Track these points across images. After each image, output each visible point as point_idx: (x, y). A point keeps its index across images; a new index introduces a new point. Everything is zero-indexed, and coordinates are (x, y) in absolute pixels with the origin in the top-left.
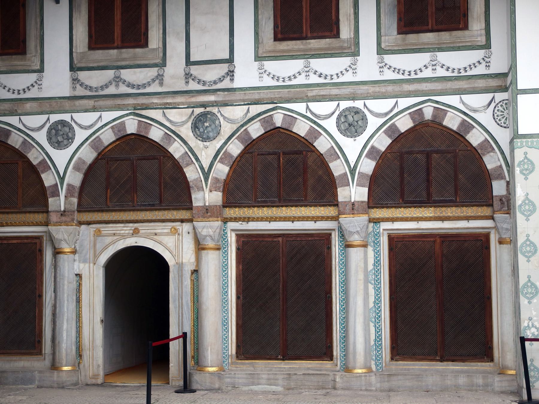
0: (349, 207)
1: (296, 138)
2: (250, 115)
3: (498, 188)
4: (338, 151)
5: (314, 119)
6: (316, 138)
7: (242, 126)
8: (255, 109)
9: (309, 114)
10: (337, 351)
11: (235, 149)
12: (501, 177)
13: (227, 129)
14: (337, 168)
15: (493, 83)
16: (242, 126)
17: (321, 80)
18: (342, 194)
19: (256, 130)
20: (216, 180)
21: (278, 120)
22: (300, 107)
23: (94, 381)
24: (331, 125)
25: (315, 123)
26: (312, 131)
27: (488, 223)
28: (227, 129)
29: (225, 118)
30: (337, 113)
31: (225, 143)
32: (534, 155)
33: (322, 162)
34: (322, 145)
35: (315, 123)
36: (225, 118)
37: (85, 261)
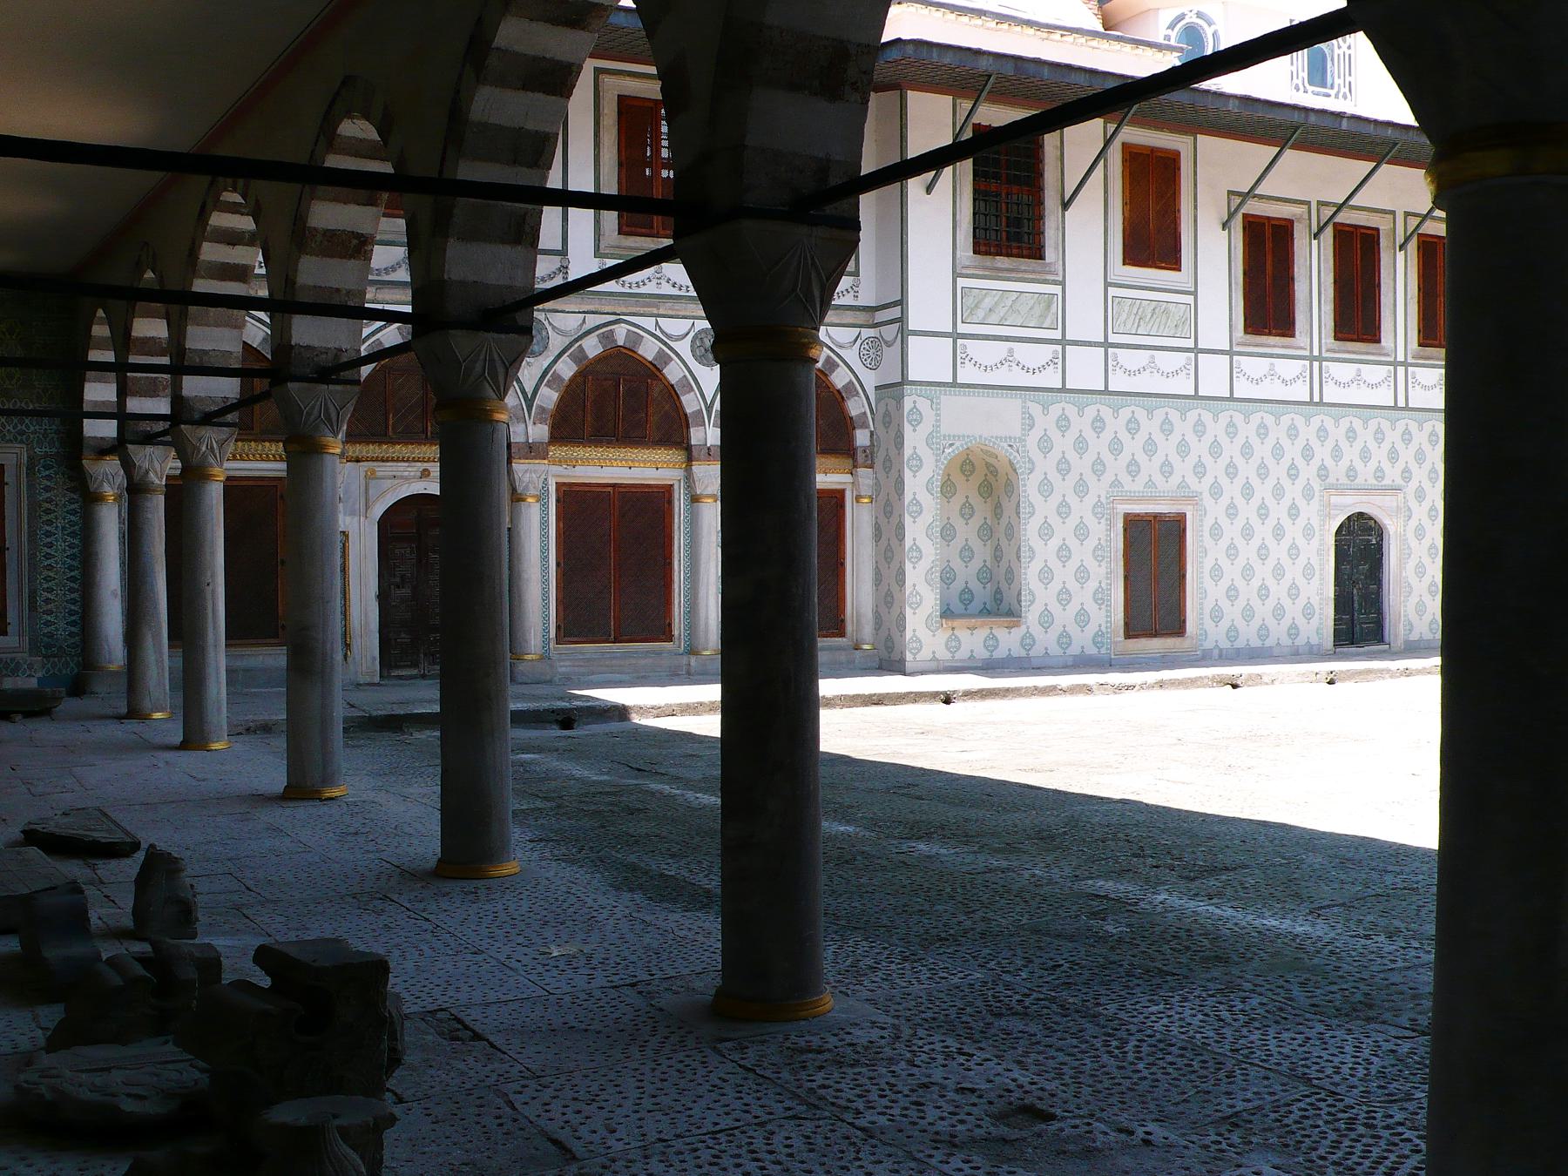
0: (705, 451)
1: (640, 363)
2: (587, 327)
3: (861, 438)
4: (690, 383)
5: (664, 339)
6: (666, 364)
7: (576, 340)
8: (593, 320)
9: (658, 333)
10: (678, 627)
11: (567, 369)
12: (865, 425)
13: (556, 343)
14: (690, 403)
15: (861, 317)
16: (576, 340)
17: (675, 292)
18: (696, 436)
19: (592, 347)
20: (542, 409)
21: (621, 334)
22: (648, 323)
23: (368, 680)
24: (684, 348)
25: (665, 344)
26: (661, 353)
27: (847, 478)
28: (556, 343)
29: (554, 328)
30: (692, 334)
31: (555, 361)
32: (924, 405)
33: (671, 394)
34: (673, 373)
35: (665, 344)
36: (554, 328)
37: (352, 513)
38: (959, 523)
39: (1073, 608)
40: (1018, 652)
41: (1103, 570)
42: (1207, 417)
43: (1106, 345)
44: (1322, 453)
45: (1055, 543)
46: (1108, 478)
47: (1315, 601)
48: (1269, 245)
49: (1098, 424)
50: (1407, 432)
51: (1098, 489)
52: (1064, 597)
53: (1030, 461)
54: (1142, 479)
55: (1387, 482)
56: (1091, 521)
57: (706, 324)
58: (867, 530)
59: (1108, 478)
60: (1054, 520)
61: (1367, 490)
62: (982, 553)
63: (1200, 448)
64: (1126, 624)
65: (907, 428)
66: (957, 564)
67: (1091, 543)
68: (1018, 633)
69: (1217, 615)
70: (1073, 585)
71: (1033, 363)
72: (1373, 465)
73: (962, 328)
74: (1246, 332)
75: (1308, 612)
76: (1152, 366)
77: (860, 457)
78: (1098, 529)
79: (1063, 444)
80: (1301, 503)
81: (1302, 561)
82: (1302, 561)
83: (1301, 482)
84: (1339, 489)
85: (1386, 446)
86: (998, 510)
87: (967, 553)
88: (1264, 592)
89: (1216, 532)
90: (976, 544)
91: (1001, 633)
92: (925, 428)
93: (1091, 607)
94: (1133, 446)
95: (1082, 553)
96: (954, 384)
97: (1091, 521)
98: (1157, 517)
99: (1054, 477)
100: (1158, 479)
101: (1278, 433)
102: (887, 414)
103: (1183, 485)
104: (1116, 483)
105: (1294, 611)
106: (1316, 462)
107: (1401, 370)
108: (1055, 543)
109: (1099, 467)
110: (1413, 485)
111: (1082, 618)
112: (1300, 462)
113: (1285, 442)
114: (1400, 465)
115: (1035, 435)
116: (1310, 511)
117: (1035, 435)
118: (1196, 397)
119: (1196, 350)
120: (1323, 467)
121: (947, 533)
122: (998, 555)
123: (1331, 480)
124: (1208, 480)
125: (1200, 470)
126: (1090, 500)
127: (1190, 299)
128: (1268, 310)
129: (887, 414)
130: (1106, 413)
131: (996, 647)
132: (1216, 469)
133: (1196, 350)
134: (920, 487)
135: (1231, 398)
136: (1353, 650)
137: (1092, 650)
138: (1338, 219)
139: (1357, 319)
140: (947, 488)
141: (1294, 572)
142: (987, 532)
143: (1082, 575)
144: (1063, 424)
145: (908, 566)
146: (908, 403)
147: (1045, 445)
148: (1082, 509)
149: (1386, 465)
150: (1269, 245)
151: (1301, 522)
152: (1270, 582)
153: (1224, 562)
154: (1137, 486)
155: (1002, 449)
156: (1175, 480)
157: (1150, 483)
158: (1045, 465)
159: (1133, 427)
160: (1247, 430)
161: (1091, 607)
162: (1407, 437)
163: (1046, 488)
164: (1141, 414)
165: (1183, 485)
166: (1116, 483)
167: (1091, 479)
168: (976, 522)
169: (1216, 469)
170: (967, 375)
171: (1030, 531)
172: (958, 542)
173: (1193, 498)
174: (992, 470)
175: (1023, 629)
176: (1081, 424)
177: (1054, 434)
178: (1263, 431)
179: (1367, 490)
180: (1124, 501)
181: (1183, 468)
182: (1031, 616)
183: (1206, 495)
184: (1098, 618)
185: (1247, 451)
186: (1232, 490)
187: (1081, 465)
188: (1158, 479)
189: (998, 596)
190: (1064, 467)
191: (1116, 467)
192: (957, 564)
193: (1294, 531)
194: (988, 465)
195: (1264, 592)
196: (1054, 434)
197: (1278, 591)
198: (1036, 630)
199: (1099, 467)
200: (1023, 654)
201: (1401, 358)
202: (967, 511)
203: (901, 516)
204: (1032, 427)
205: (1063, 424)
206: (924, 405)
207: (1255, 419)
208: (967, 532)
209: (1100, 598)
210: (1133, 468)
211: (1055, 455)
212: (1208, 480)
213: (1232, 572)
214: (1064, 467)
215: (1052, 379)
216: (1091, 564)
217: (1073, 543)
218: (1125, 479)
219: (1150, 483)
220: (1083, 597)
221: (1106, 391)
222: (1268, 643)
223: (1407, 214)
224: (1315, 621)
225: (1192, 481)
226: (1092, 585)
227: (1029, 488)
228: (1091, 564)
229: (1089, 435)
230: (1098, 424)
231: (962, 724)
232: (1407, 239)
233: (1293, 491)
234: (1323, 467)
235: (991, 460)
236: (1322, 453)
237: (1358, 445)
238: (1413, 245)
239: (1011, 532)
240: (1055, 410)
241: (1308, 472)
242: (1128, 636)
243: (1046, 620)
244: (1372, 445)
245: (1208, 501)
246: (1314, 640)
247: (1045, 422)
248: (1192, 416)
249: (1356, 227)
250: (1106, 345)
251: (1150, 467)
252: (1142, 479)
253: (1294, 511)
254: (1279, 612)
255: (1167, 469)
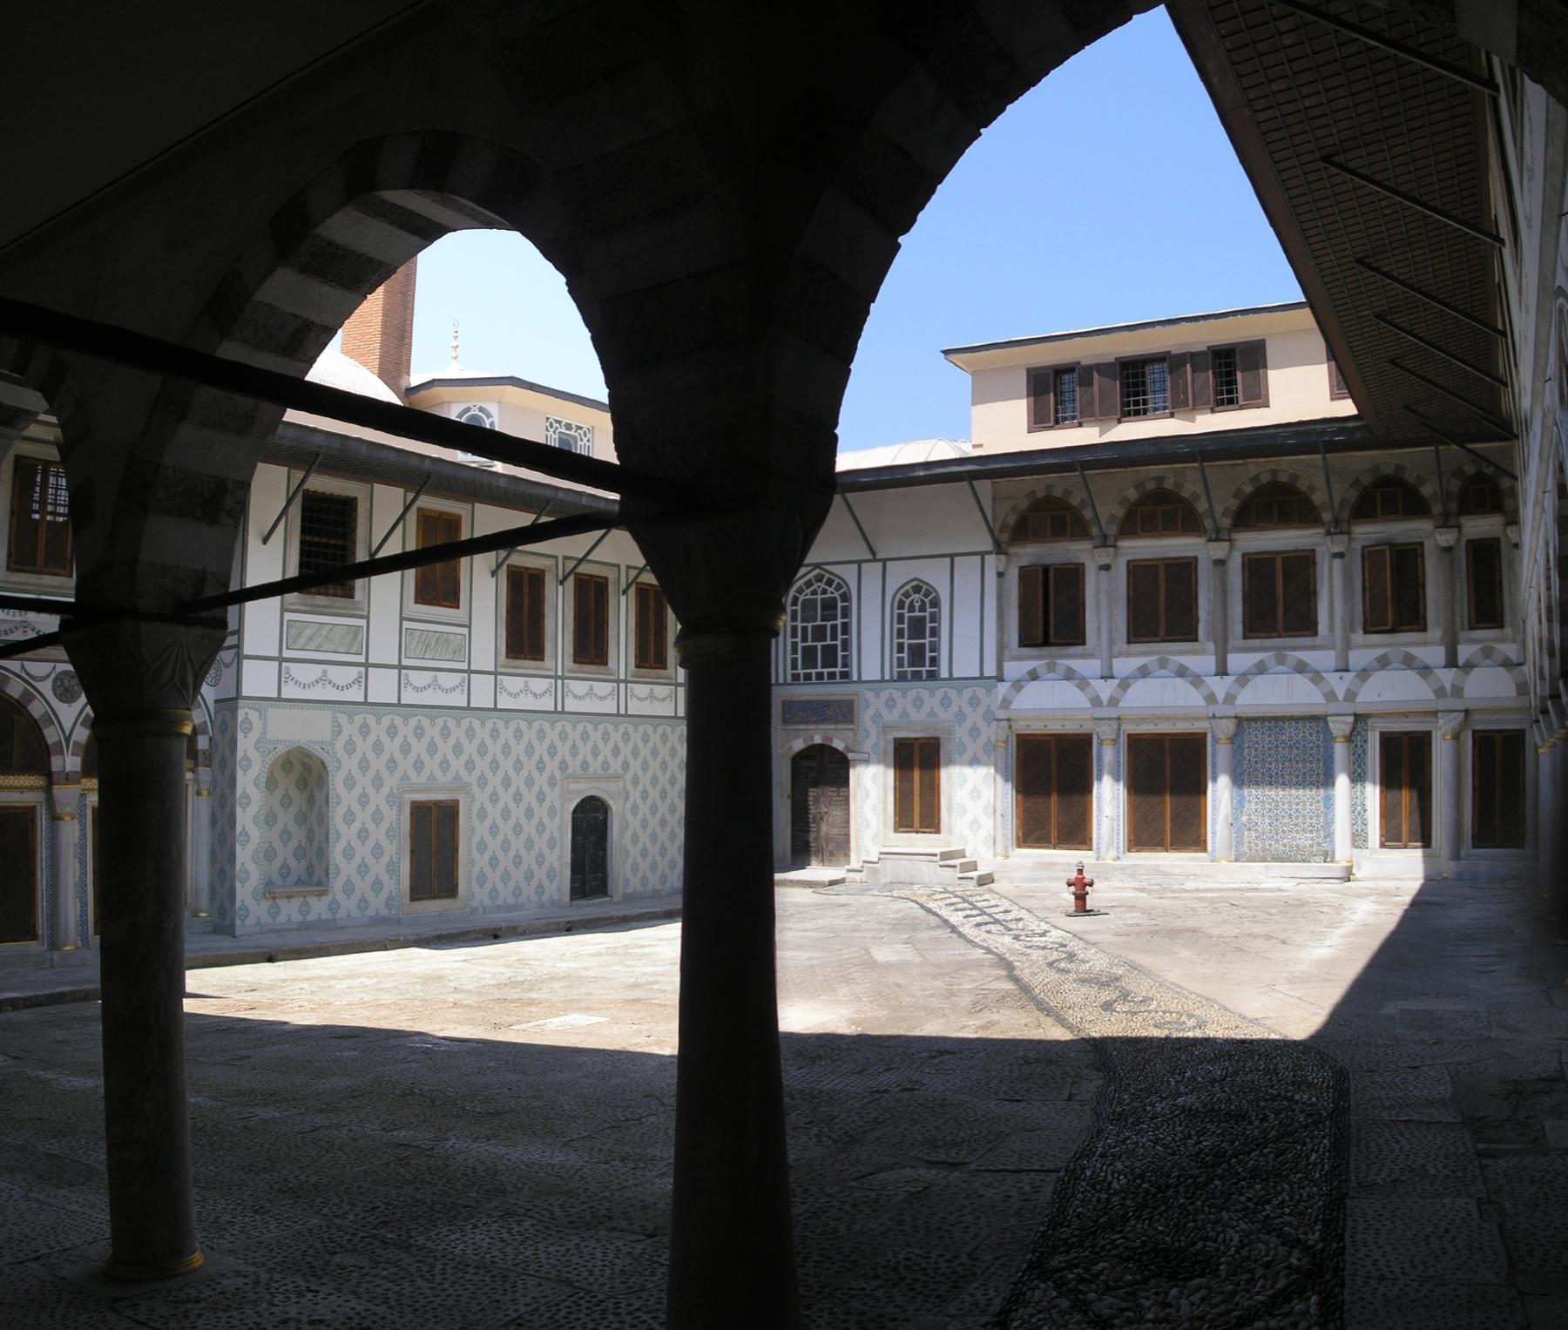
3: (202, 743)
12: (205, 732)
38: (279, 811)
39: (370, 878)
40: (326, 915)
41: (394, 847)
42: (476, 724)
43: (400, 667)
44: (563, 750)
45: (356, 826)
46: (399, 773)
47: (556, 865)
48: (526, 589)
49: (392, 731)
50: (626, 733)
51: (391, 782)
52: (363, 869)
53: (338, 761)
54: (426, 773)
55: (611, 771)
56: (385, 808)
57: (69, 667)
58: (205, 818)
59: (399, 773)
60: (356, 808)
61: (597, 778)
62: (299, 835)
63: (470, 748)
64: (412, 889)
65: (240, 736)
66: (277, 844)
67: (385, 825)
68: (325, 900)
69: (482, 879)
70: (370, 860)
71: (342, 682)
72: (601, 759)
73: (287, 654)
74: (507, 657)
75: (551, 875)
76: (435, 685)
77: (201, 758)
78: (390, 815)
79: (364, 747)
80: (546, 789)
81: (547, 835)
82: (547, 835)
83: (547, 773)
84: (575, 778)
85: (611, 744)
86: (311, 800)
87: (286, 835)
88: (517, 860)
89: (482, 814)
90: (293, 827)
91: (312, 901)
92: (254, 735)
93: (385, 877)
94: (419, 747)
95: (378, 834)
96: (279, 699)
97: (385, 808)
98: (437, 803)
99: (356, 773)
100: (438, 773)
101: (530, 735)
102: (224, 723)
103: (457, 777)
104: (406, 777)
105: (540, 874)
106: (558, 758)
107: (622, 686)
108: (356, 826)
109: (392, 765)
110: (630, 774)
111: (377, 886)
112: (546, 758)
113: (535, 743)
114: (621, 759)
115: (343, 738)
116: (553, 796)
117: (343, 738)
118: (468, 708)
119: (470, 672)
120: (563, 762)
121: (270, 819)
122: (310, 837)
123: (570, 771)
124: (476, 773)
125: (470, 766)
126: (385, 791)
127: (465, 631)
128: (524, 639)
129: (224, 723)
130: (398, 721)
131: (308, 912)
132: (482, 765)
133: (470, 672)
134: (249, 782)
135: (495, 709)
136: (585, 902)
137: (384, 912)
138: (579, 570)
139: (590, 647)
140: (271, 784)
141: (541, 844)
142: (302, 818)
143: (377, 851)
144: (365, 730)
145: (238, 848)
146: (241, 714)
147: (350, 747)
148: (378, 799)
149: (610, 759)
150: (526, 589)
151: (547, 804)
152: (523, 853)
153: (488, 838)
154: (422, 779)
155: (316, 750)
156: (450, 775)
157: (432, 777)
158: (350, 764)
159: (419, 732)
160: (507, 734)
161: (385, 877)
162: (626, 737)
163: (350, 783)
164: (425, 722)
165: (457, 777)
166: (406, 777)
167: (385, 774)
168: (293, 810)
169: (482, 765)
170: (289, 692)
171: (337, 816)
172: (279, 827)
173: (465, 788)
174: (307, 768)
175: (330, 897)
176: (379, 730)
177: (358, 739)
178: (518, 735)
179: (597, 778)
180: (410, 792)
181: (457, 765)
182: (337, 885)
183: (475, 785)
184: (389, 885)
185: (506, 750)
186: (495, 781)
187: (377, 763)
188: (438, 773)
189: (310, 870)
190: (364, 765)
191: (405, 764)
192: (277, 844)
193: (541, 812)
194: (304, 764)
195: (517, 860)
196: (358, 739)
197: (529, 859)
198: (340, 897)
199: (392, 765)
200: (330, 916)
201: (622, 677)
202: (286, 801)
203: (233, 807)
204: (340, 733)
205: (365, 730)
206: (254, 716)
207: (513, 725)
208: (286, 818)
209: (392, 869)
210: (419, 765)
211: (357, 756)
212: (476, 773)
213: (494, 845)
214: (364, 765)
215: (356, 695)
216: (384, 842)
217: (371, 826)
218: (412, 773)
219: (432, 777)
220: (378, 868)
221: (399, 704)
222: (522, 899)
223: (629, 567)
224: (556, 881)
225: (464, 774)
226: (385, 859)
227: (337, 782)
228: (384, 842)
229: (385, 739)
230: (392, 731)
231: (284, 981)
232: (629, 586)
233: (541, 781)
234: (563, 762)
235: (307, 760)
236: (563, 750)
237: (590, 744)
238: (632, 591)
239: (323, 818)
240: (359, 720)
241: (552, 766)
242: (413, 899)
243: (349, 888)
244: (600, 743)
245: (476, 790)
246: (556, 897)
247: (350, 729)
248: (465, 723)
249: (591, 576)
250: (400, 667)
251: (431, 765)
252: (426, 773)
253: (541, 797)
254: (529, 875)
255: (445, 765)
